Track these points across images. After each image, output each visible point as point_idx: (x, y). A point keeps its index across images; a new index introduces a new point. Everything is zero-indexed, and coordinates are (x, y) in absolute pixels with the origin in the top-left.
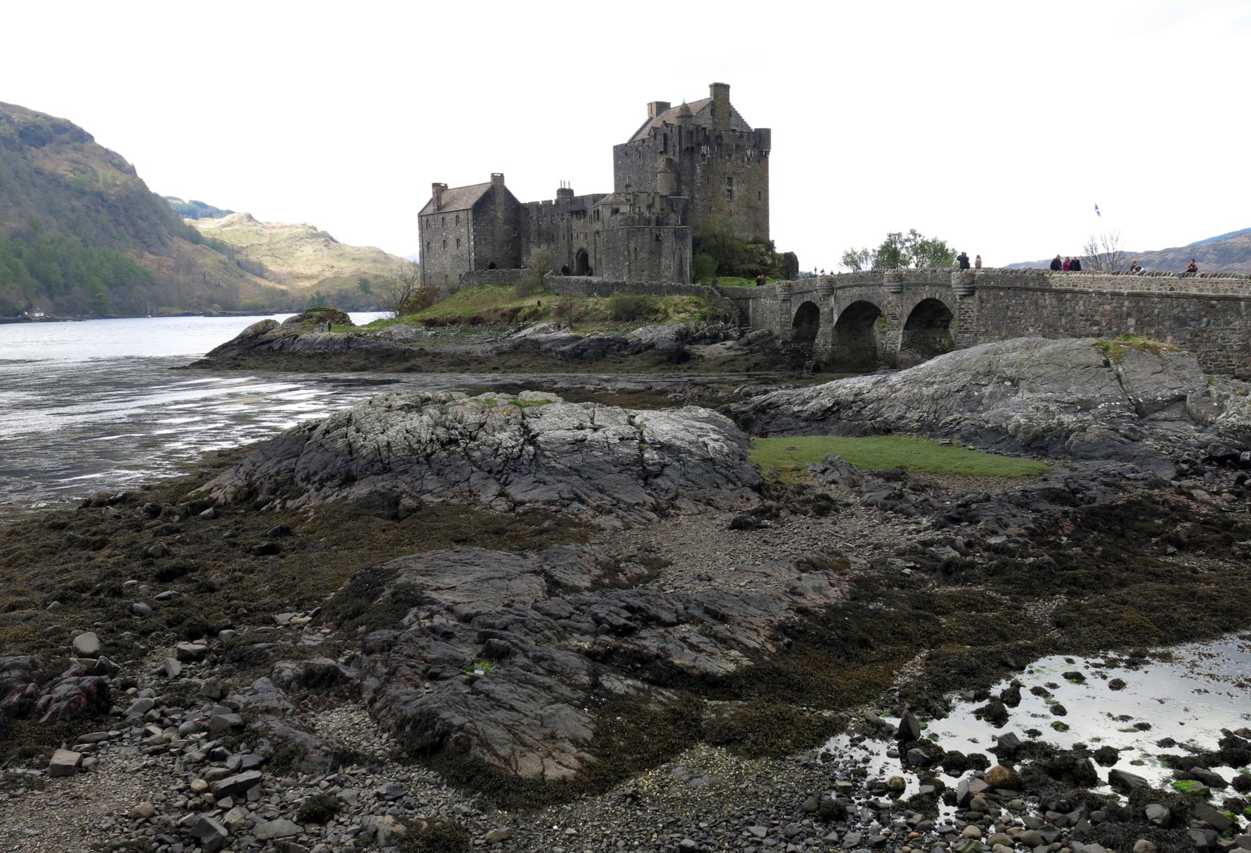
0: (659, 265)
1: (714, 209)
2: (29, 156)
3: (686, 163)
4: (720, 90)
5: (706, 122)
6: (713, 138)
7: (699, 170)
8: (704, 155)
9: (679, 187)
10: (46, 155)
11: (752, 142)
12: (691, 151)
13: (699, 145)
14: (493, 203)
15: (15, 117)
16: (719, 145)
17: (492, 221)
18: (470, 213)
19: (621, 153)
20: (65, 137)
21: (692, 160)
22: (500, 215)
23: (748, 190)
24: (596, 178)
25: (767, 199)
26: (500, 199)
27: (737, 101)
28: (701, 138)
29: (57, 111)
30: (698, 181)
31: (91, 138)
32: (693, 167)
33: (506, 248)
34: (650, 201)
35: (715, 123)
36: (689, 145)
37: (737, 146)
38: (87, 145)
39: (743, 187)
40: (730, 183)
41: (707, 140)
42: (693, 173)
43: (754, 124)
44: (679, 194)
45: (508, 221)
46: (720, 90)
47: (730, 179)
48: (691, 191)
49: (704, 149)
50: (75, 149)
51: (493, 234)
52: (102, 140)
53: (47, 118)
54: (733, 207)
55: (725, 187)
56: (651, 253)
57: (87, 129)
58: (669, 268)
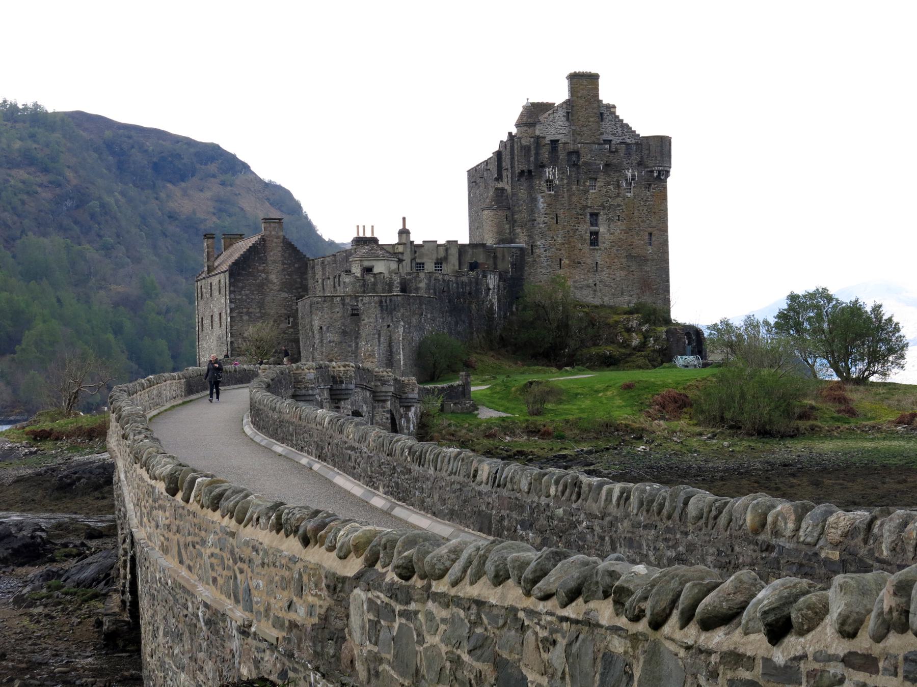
0: (356, 353)
1: (565, 261)
2: (163, 195)
3: (522, 193)
4: (584, 84)
5: (554, 129)
6: (562, 155)
7: (541, 204)
8: (549, 181)
9: (512, 231)
10: (185, 193)
11: (635, 158)
12: (527, 175)
13: (543, 166)
14: (263, 261)
15: (150, 145)
16: (575, 165)
17: (261, 287)
18: (227, 274)
19: (476, 176)
20: (212, 167)
21: (531, 188)
22: (273, 277)
23: (628, 231)
24: (446, 219)
25: (665, 243)
26: (275, 254)
27: (606, 95)
28: (545, 154)
29: (201, 134)
30: (541, 219)
31: (245, 167)
32: (534, 200)
33: (283, 326)
34: (442, 254)
35: (575, 133)
36: (525, 168)
37: (607, 165)
38: (241, 178)
39: (618, 228)
40: (594, 223)
41: (554, 161)
42: (532, 211)
43: (644, 128)
44: (512, 242)
45: (287, 286)
46: (584, 84)
47: (595, 215)
48: (530, 236)
49: (549, 172)
50: (223, 184)
51: (261, 305)
52: (252, 169)
53: (189, 142)
54: (600, 257)
55: (585, 228)
56: (344, 333)
57: (241, 157)
58: (372, 355)
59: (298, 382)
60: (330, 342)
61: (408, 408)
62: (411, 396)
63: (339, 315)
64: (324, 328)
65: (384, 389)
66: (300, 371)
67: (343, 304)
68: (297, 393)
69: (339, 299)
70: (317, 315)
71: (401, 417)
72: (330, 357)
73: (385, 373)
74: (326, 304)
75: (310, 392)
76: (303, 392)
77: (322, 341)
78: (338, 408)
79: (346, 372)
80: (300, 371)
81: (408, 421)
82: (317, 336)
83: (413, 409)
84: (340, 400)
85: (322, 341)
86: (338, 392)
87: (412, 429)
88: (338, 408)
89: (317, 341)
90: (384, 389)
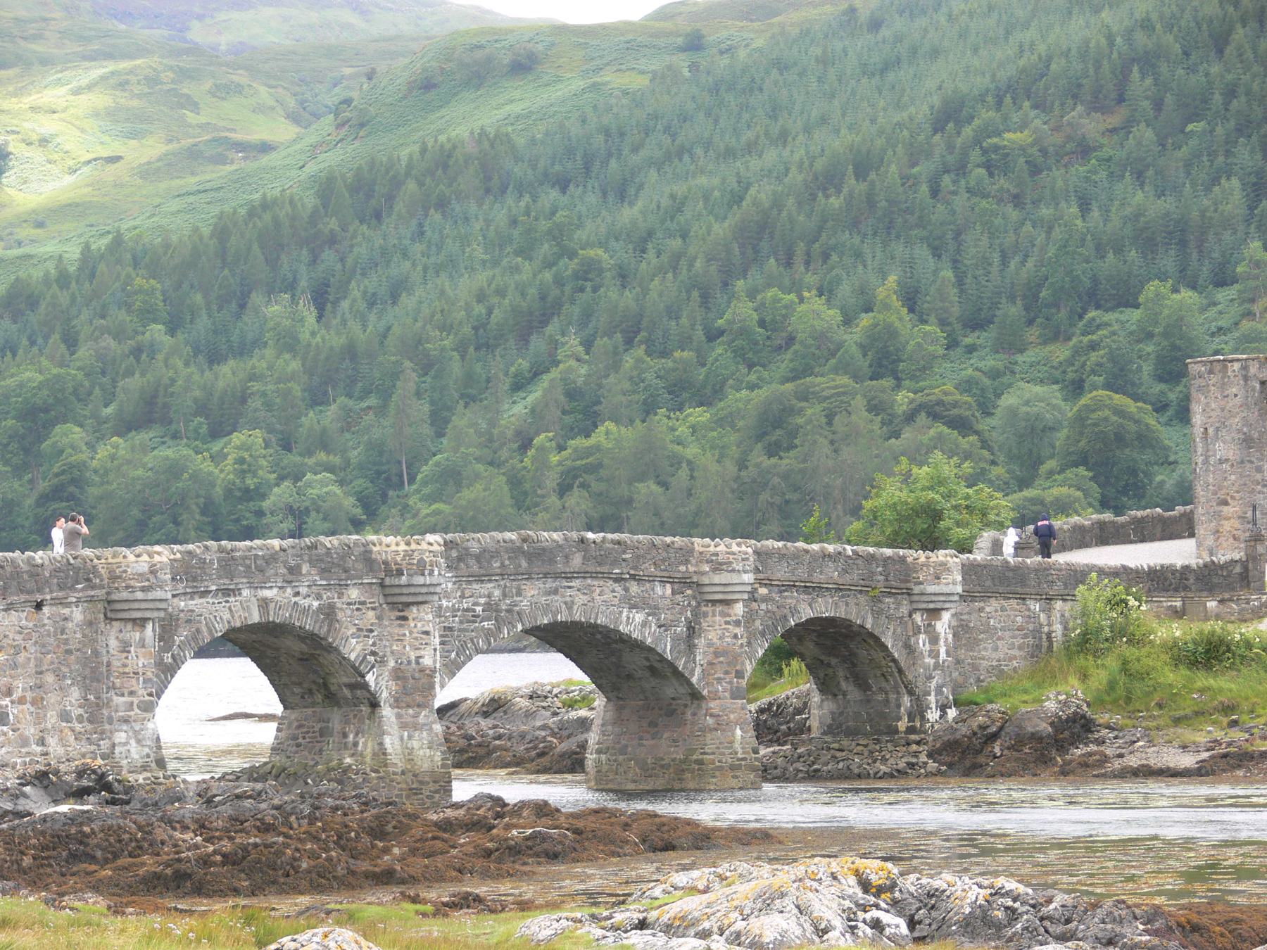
59: (114, 578)
60: (1221, 461)
61: (935, 613)
62: (931, 589)
63: (1238, 400)
64: (1210, 431)
65: (717, 579)
66: (120, 559)
67: (1246, 378)
68: (114, 597)
69: (1237, 366)
70: (1199, 402)
71: (917, 631)
72: (1221, 495)
73: (722, 548)
74: (1214, 379)
75: (139, 595)
76: (125, 595)
77: (1206, 462)
78: (405, 618)
79: (408, 554)
80: (120, 559)
81: (934, 640)
82: (1200, 450)
83: (946, 616)
84: (408, 605)
85: (1207, 458)
86: (397, 591)
87: (943, 655)
88: (405, 618)
89: (1200, 460)
90: (717, 579)
